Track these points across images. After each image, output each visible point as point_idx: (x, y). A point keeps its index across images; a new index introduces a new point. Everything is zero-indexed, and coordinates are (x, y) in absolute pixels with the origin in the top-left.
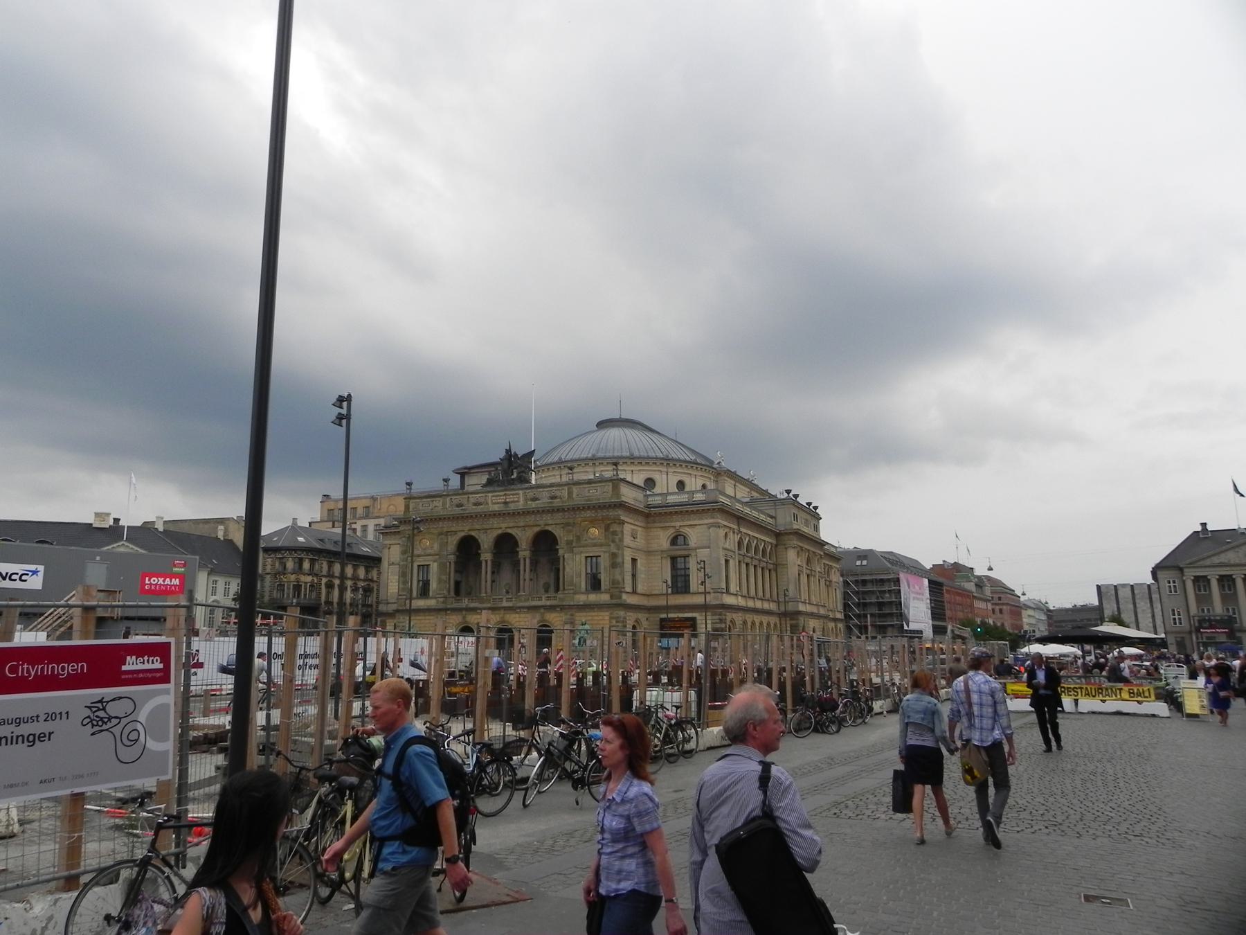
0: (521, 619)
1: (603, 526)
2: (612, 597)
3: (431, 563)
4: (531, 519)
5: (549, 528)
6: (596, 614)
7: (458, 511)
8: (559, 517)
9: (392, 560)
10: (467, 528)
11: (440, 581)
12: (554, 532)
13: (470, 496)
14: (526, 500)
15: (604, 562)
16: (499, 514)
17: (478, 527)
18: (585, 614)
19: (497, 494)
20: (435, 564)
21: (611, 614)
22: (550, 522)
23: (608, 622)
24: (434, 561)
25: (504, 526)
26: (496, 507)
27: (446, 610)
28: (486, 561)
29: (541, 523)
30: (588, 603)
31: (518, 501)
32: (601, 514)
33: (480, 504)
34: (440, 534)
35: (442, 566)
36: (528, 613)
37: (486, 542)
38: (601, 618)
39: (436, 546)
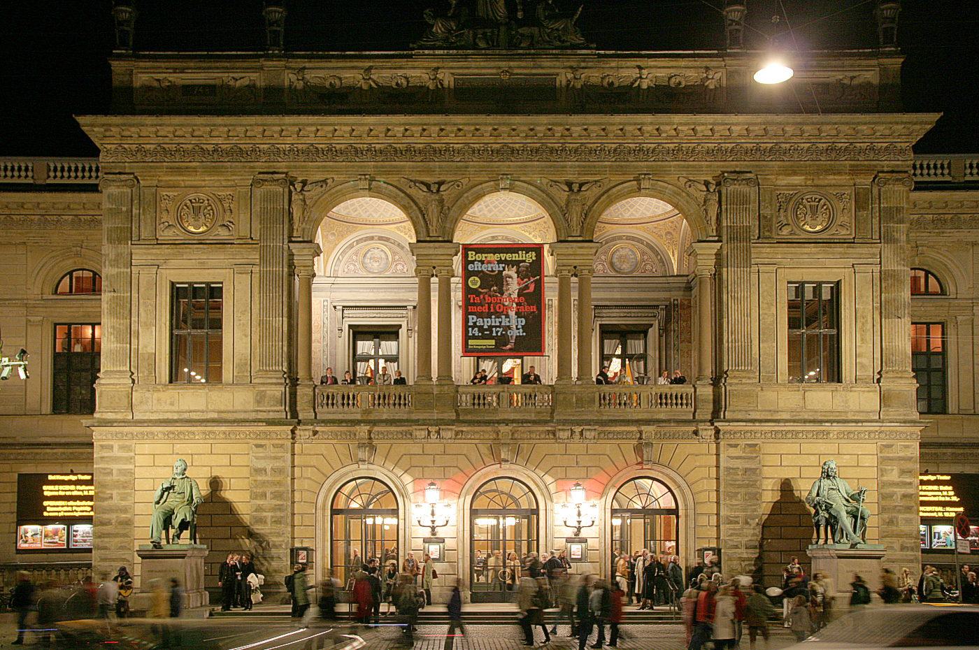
23: (873, 473)
38: (846, 460)
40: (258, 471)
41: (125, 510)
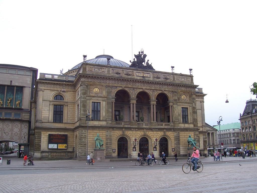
0: (154, 134)
1: (188, 95)
2: (194, 126)
4: (158, 87)
5: (166, 92)
6: (188, 133)
7: (117, 75)
8: (170, 88)
9: (45, 98)
10: (124, 86)
11: (107, 111)
12: (168, 94)
13: (124, 70)
14: (154, 77)
15: (190, 110)
16: (143, 82)
17: (130, 86)
18: (184, 133)
19: (139, 71)
20: (104, 103)
21: (195, 133)
22: (167, 90)
23: (193, 137)
24: (103, 101)
25: (145, 88)
26: (139, 78)
27: (113, 128)
28: (133, 104)
29: (163, 89)
30: (185, 128)
31: (150, 77)
32: (188, 89)
33: (130, 75)
35: (108, 103)
36: (157, 131)
37: (133, 94)
39: (104, 93)
40: (107, 136)
41: (85, 142)
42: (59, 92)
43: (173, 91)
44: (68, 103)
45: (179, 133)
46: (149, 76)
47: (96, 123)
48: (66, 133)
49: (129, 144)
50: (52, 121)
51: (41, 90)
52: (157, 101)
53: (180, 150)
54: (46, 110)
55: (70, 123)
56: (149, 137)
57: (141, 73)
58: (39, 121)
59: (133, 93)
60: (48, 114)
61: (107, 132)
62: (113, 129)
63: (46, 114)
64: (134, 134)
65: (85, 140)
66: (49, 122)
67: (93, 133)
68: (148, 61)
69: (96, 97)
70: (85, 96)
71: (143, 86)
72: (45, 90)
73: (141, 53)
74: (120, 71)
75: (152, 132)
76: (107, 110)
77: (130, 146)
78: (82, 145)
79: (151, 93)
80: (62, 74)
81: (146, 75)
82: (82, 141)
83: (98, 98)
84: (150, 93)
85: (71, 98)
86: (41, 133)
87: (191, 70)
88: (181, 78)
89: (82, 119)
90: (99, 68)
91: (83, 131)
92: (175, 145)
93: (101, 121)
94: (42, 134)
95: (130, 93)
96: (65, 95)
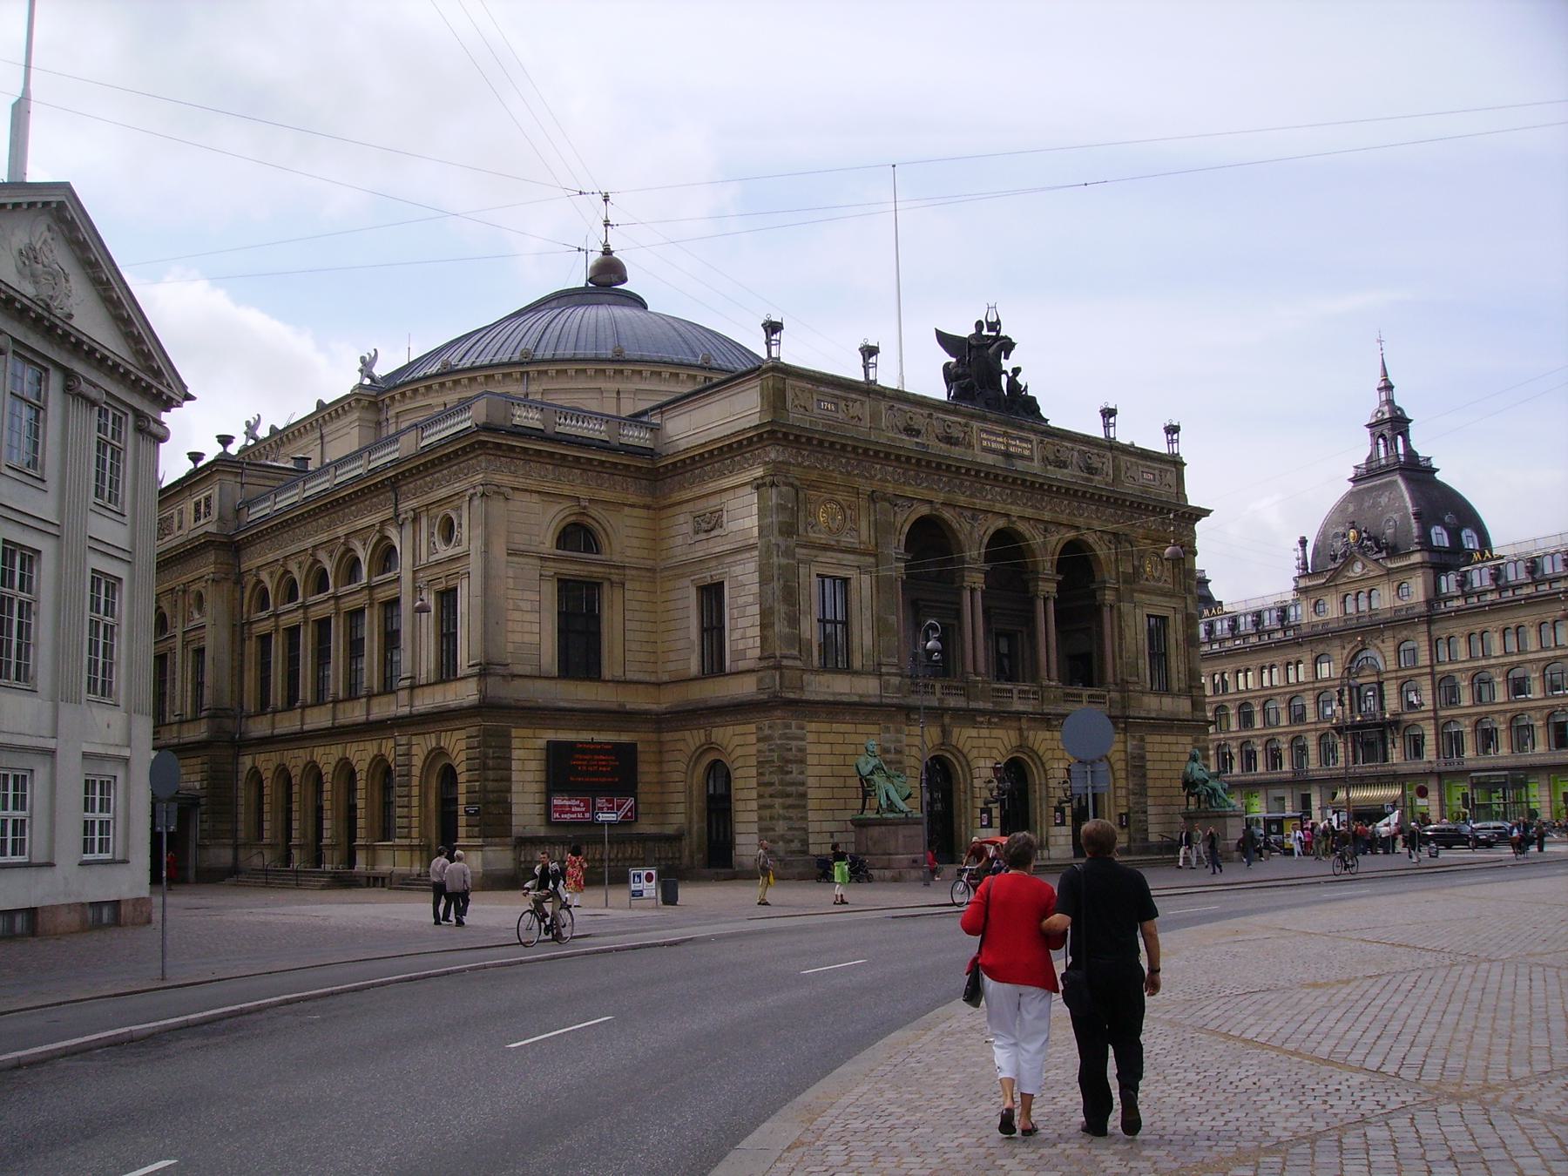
3: (852, 574)
7: (908, 442)
9: (520, 541)
10: (940, 497)
11: (881, 627)
17: (962, 500)
19: (988, 426)
20: (866, 578)
22: (1096, 525)
25: (1018, 511)
26: (990, 459)
27: (907, 712)
28: (973, 590)
29: (1080, 521)
34: (873, 497)
35: (880, 585)
37: (973, 539)
42: (585, 508)
43: (1115, 534)
44: (627, 572)
45: (1142, 739)
46: (1027, 453)
47: (839, 686)
48: (625, 738)
49: (965, 792)
50: (555, 672)
51: (499, 493)
52: (1060, 578)
53: (1146, 821)
54: (526, 606)
55: (647, 683)
56: (1037, 760)
57: (998, 435)
58: (500, 670)
59: (971, 534)
60: (536, 628)
61: (887, 729)
62: (908, 716)
63: (527, 627)
64: (982, 740)
65: (802, 773)
66: (540, 677)
67: (830, 738)
68: (1016, 371)
69: (834, 550)
70: (792, 541)
71: (1012, 503)
72: (518, 495)
73: (989, 331)
74: (919, 422)
75: (1048, 735)
76: (879, 620)
77: (969, 802)
78: (790, 801)
79: (1040, 540)
80: (367, 381)
81: (1015, 446)
82: (788, 778)
83: (840, 555)
84: (1035, 537)
85: (635, 543)
86: (508, 736)
87: (1172, 430)
88: (1141, 469)
89: (785, 662)
90: (836, 397)
91: (788, 726)
92: (1131, 797)
93: (856, 673)
94: (515, 743)
95: (962, 537)
96: (607, 525)
